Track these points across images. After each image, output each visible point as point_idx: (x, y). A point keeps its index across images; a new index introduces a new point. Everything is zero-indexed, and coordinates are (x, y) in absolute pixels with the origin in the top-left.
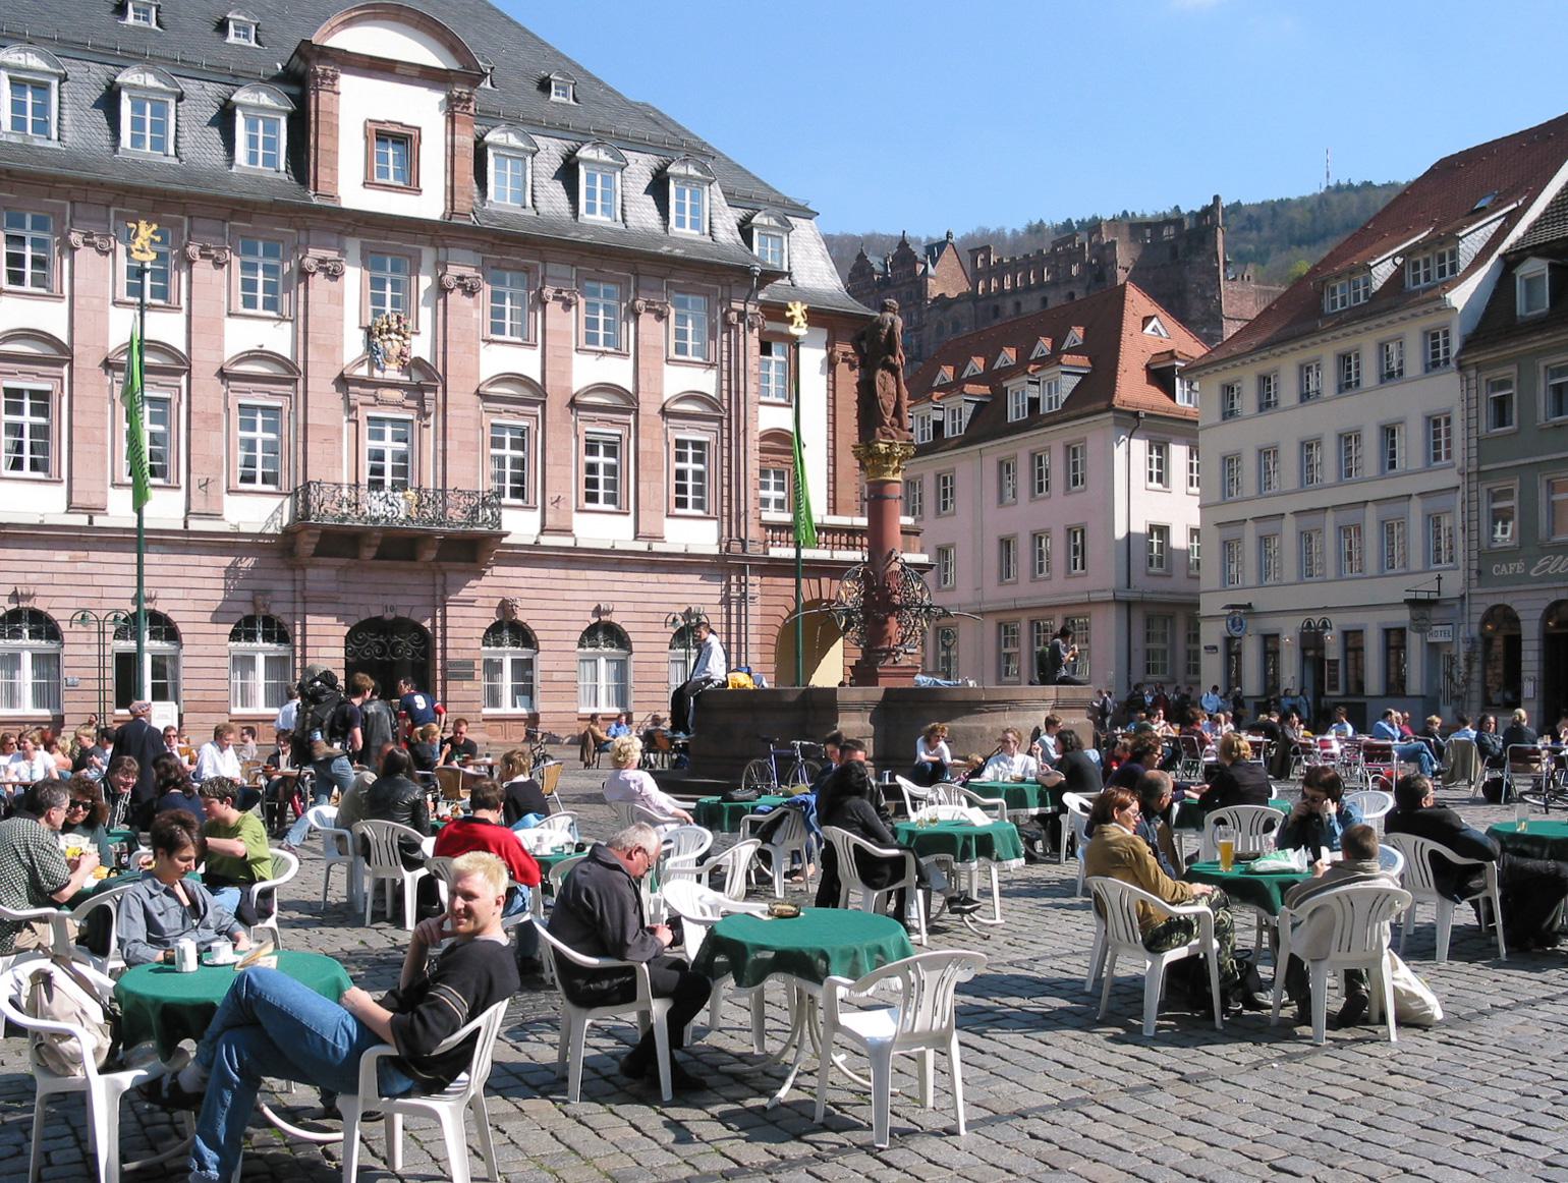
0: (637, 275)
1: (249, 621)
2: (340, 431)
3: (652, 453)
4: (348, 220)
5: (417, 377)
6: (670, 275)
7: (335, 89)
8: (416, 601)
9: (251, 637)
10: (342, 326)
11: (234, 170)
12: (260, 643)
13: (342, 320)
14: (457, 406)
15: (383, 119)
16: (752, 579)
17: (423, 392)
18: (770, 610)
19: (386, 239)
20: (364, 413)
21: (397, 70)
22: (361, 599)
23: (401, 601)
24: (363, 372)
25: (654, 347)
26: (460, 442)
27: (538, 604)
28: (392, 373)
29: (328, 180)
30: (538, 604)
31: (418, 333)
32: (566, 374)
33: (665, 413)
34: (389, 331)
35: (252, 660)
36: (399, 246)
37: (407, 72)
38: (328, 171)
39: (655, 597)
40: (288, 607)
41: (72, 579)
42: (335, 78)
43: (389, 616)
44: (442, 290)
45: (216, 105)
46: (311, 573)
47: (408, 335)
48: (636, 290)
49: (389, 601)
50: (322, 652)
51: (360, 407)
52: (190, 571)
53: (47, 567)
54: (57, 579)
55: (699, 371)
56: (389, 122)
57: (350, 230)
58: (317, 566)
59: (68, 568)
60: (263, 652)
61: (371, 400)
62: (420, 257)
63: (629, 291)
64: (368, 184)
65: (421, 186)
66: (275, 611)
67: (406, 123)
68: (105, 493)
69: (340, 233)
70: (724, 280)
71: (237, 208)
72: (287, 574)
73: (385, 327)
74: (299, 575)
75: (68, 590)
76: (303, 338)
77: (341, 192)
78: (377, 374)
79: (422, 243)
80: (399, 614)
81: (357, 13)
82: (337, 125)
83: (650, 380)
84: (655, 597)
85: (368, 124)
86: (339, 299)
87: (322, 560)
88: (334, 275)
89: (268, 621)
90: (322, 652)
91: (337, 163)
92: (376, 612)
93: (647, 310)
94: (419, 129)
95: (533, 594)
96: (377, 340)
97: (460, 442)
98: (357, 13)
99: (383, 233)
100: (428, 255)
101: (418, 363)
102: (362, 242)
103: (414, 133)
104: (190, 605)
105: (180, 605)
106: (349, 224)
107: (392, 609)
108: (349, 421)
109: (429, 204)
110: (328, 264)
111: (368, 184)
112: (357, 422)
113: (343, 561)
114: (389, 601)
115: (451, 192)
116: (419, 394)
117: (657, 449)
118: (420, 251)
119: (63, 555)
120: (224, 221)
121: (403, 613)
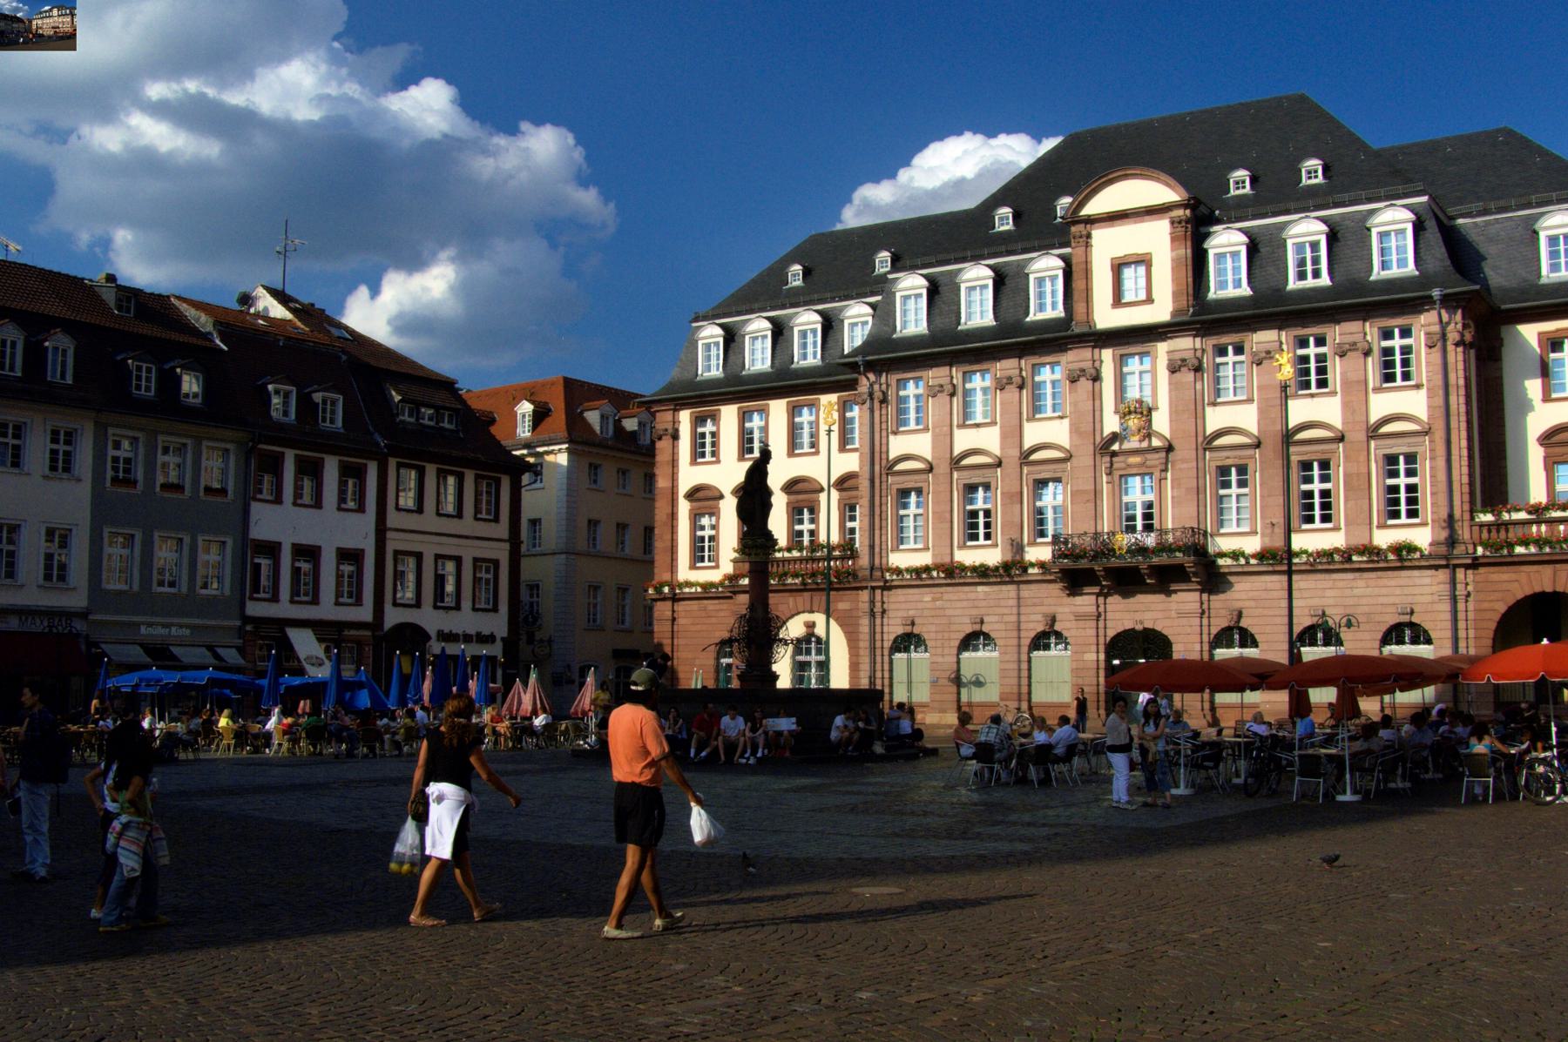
2: (1096, 493)
3: (1358, 475)
8: (1160, 615)
18: (1486, 605)
24: (1116, 447)
27: (1258, 612)
30: (1258, 612)
34: (1130, 413)
39: (1364, 601)
41: (933, 613)
42: (1089, 236)
43: (1139, 627)
52: (1003, 603)
53: (920, 606)
54: (926, 613)
59: (929, 606)
61: (1123, 465)
68: (952, 554)
75: (931, 620)
76: (1075, 430)
84: (1364, 601)
86: (1096, 396)
92: (1128, 625)
95: (1252, 604)
100: (1162, 348)
103: (1148, 257)
104: (1002, 627)
105: (996, 626)
107: (1141, 622)
109: (1161, 311)
113: (1096, 589)
114: (1138, 616)
115: (1176, 295)
119: (928, 598)
121: (1149, 625)
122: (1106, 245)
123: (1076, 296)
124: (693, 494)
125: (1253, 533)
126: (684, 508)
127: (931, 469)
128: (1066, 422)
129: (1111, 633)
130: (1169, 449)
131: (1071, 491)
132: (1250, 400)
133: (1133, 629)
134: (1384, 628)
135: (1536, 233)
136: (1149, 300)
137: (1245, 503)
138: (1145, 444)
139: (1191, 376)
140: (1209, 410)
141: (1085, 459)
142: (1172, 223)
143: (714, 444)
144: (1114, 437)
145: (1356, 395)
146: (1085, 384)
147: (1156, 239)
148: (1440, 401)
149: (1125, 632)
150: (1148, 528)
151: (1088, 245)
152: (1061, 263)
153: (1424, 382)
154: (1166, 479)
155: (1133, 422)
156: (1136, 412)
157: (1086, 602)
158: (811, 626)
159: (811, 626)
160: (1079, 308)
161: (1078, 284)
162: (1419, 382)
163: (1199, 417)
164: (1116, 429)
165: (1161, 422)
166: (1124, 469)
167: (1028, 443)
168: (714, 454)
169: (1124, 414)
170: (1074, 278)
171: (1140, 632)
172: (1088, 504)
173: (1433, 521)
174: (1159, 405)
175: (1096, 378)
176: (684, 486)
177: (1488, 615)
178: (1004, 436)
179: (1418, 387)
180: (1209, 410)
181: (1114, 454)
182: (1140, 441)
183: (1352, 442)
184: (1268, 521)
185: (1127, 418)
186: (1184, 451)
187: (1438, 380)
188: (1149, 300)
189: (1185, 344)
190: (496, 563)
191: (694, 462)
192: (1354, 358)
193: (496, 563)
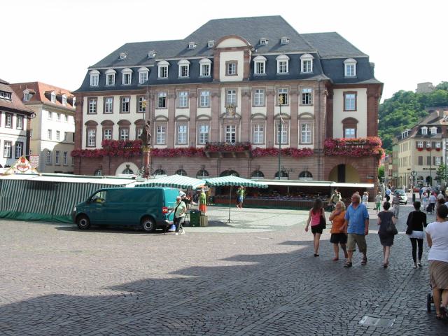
1: (202, 171)
2: (219, 131)
16: (321, 159)
28: (230, 116)
42: (219, 54)
46: (212, 161)
76: (212, 111)
86: (219, 102)
89: (206, 172)
100: (240, 89)
111: (227, 75)
115: (244, 74)
121: (233, 169)
122: (224, 58)
123: (215, 72)
124: (87, 124)
125: (264, 144)
126: (84, 128)
127: (168, 120)
130: (241, 118)
132: (264, 106)
134: (300, 172)
135: (344, 65)
137: (262, 135)
139: (248, 98)
140: (252, 108)
141: (215, 120)
143: (95, 108)
145: (295, 107)
146: (216, 98)
147: (239, 57)
148: (317, 110)
150: (233, 141)
151: (219, 57)
157: (214, 162)
158: (128, 166)
159: (128, 166)
160: (215, 75)
161: (215, 68)
163: (250, 109)
164: (225, 111)
165: (238, 110)
167: (198, 114)
168: (95, 111)
169: (228, 108)
170: (214, 66)
175: (219, 97)
176: (85, 121)
178: (191, 112)
179: (312, 105)
180: (252, 108)
181: (224, 119)
186: (245, 119)
187: (317, 104)
189: (247, 88)
190: (22, 143)
191: (88, 113)
192: (294, 96)
193: (22, 143)
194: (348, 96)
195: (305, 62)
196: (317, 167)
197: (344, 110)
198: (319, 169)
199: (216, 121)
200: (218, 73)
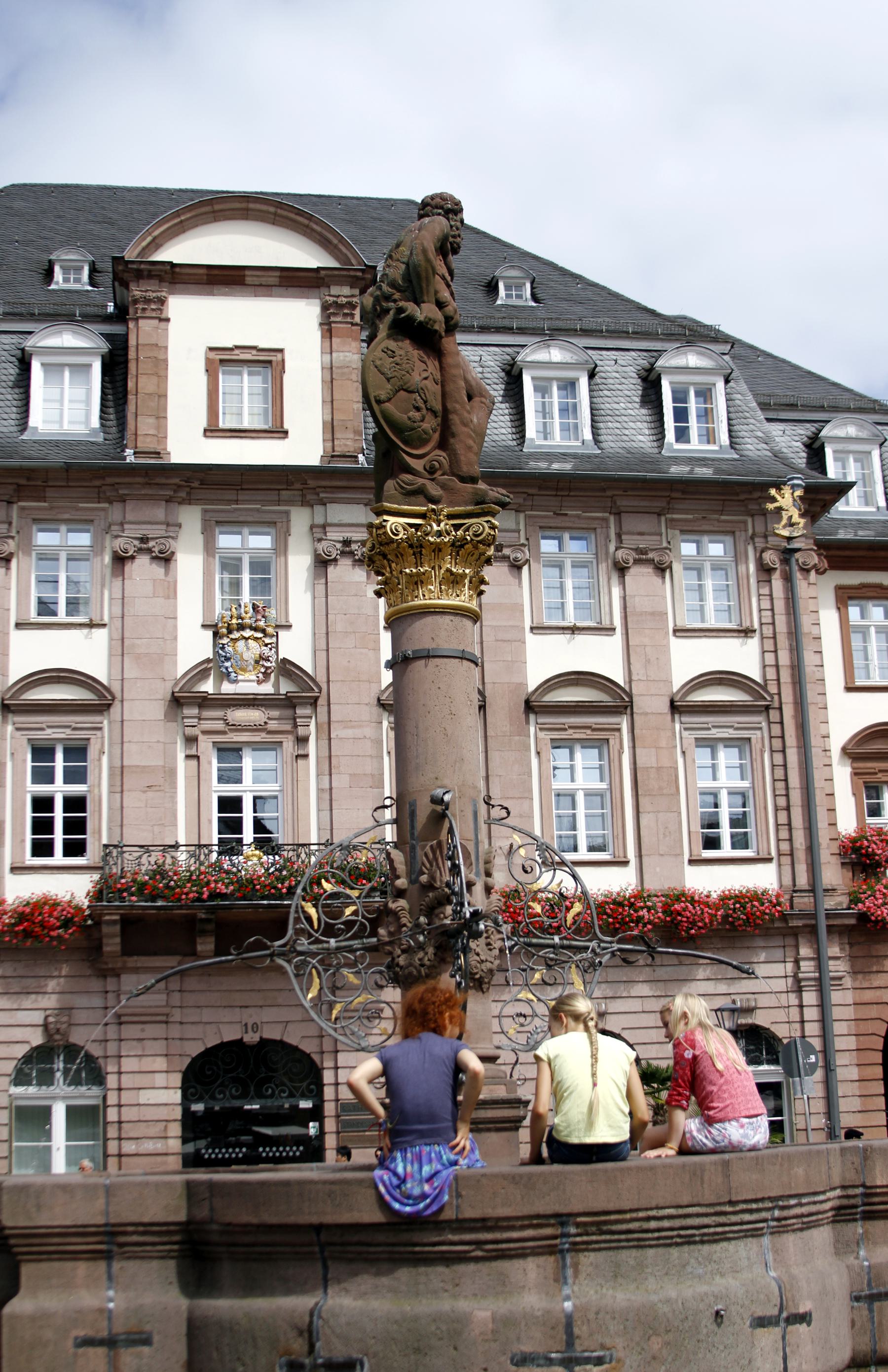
0: (618, 514)
2: (172, 773)
3: (659, 769)
4: (176, 481)
5: (286, 687)
6: (670, 510)
7: (163, 316)
9: (46, 1079)
10: (175, 627)
11: (25, 437)
12: (60, 1087)
13: (175, 618)
14: (347, 724)
15: (230, 346)
17: (294, 707)
18: (868, 996)
19: (237, 502)
20: (206, 746)
21: (248, 280)
22: (207, 1015)
23: (268, 1015)
24: (208, 686)
25: (653, 614)
26: (352, 775)
29: (151, 432)
31: (289, 627)
32: (519, 662)
33: (675, 708)
34: (241, 627)
35: (45, 1114)
36: (258, 510)
37: (263, 281)
38: (151, 420)
40: (97, 1032)
42: (162, 301)
43: (251, 1038)
44: (322, 563)
45: (14, 359)
46: (130, 982)
47: (270, 630)
48: (619, 536)
49: (252, 1016)
50: (145, 1097)
51: (201, 738)
55: (733, 644)
56: (237, 347)
57: (183, 494)
58: (136, 970)
60: (64, 1098)
61: (220, 725)
62: (289, 521)
63: (607, 538)
64: (212, 431)
65: (286, 426)
66: (77, 1037)
67: (262, 345)
69: (169, 500)
70: (753, 507)
71: (23, 482)
72: (96, 984)
73: (234, 621)
74: (111, 983)
77: (170, 447)
78: (227, 688)
79: (291, 502)
80: (266, 1035)
81: (188, 215)
82: (166, 361)
83: (648, 661)
85: (213, 355)
86: (171, 592)
87: (133, 961)
88: (166, 559)
90: (145, 1097)
91: (165, 409)
92: (230, 1034)
93: (637, 562)
94: (281, 351)
96: (225, 641)
97: (352, 775)
98: (188, 215)
99: (231, 495)
101: (287, 668)
102: (205, 511)
106: (179, 486)
107: (255, 1027)
108: (188, 757)
110: (151, 544)
111: (212, 431)
112: (198, 757)
113: (171, 962)
115: (331, 429)
116: (288, 712)
117: (666, 763)
118: (287, 513)
120: (10, 503)
121: (272, 1033)
128: (101, 635)
129: (196, 1049)
131: (111, 768)
133: (240, 1042)
136: (279, 432)
138: (267, 688)
142: (325, 307)
144: (201, 671)
148: (784, 658)
149: (223, 1046)
152: (104, 346)
153: (756, 626)
154: (306, 756)
155: (249, 650)
156: (256, 629)
162: (746, 624)
166: (223, 733)
171: (252, 1047)
172: (150, 794)
173: (780, 855)
174: (292, 620)
177: (873, 1012)
181: (204, 702)
182: (259, 682)
183: (646, 714)
184: (506, 845)
185: (236, 635)
188: (279, 432)
194: (854, 612)
195: (680, 396)
196: (810, 997)
197: (850, 689)
198: (823, 1006)
199: (157, 710)
200: (161, 416)
